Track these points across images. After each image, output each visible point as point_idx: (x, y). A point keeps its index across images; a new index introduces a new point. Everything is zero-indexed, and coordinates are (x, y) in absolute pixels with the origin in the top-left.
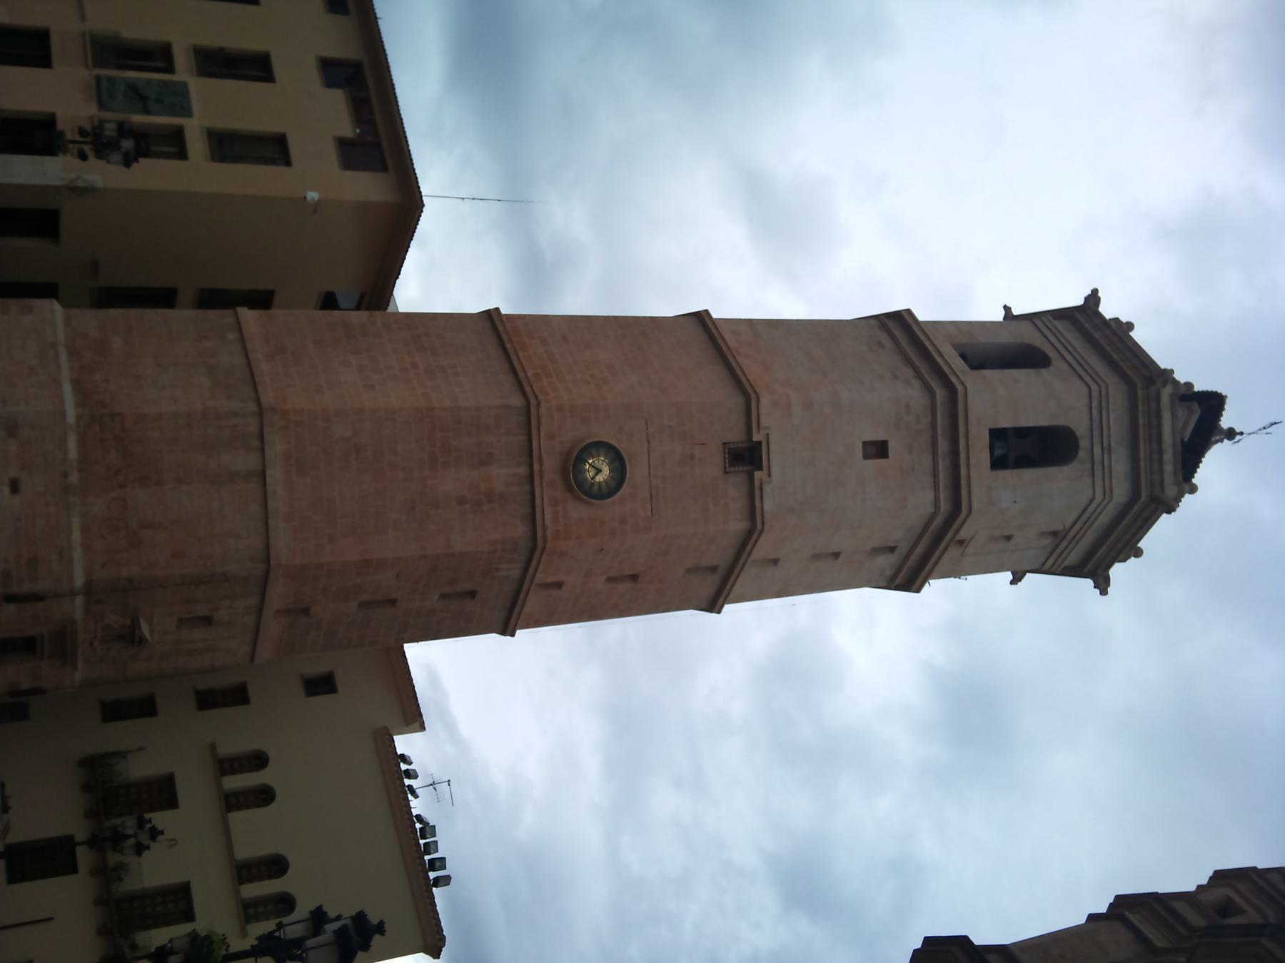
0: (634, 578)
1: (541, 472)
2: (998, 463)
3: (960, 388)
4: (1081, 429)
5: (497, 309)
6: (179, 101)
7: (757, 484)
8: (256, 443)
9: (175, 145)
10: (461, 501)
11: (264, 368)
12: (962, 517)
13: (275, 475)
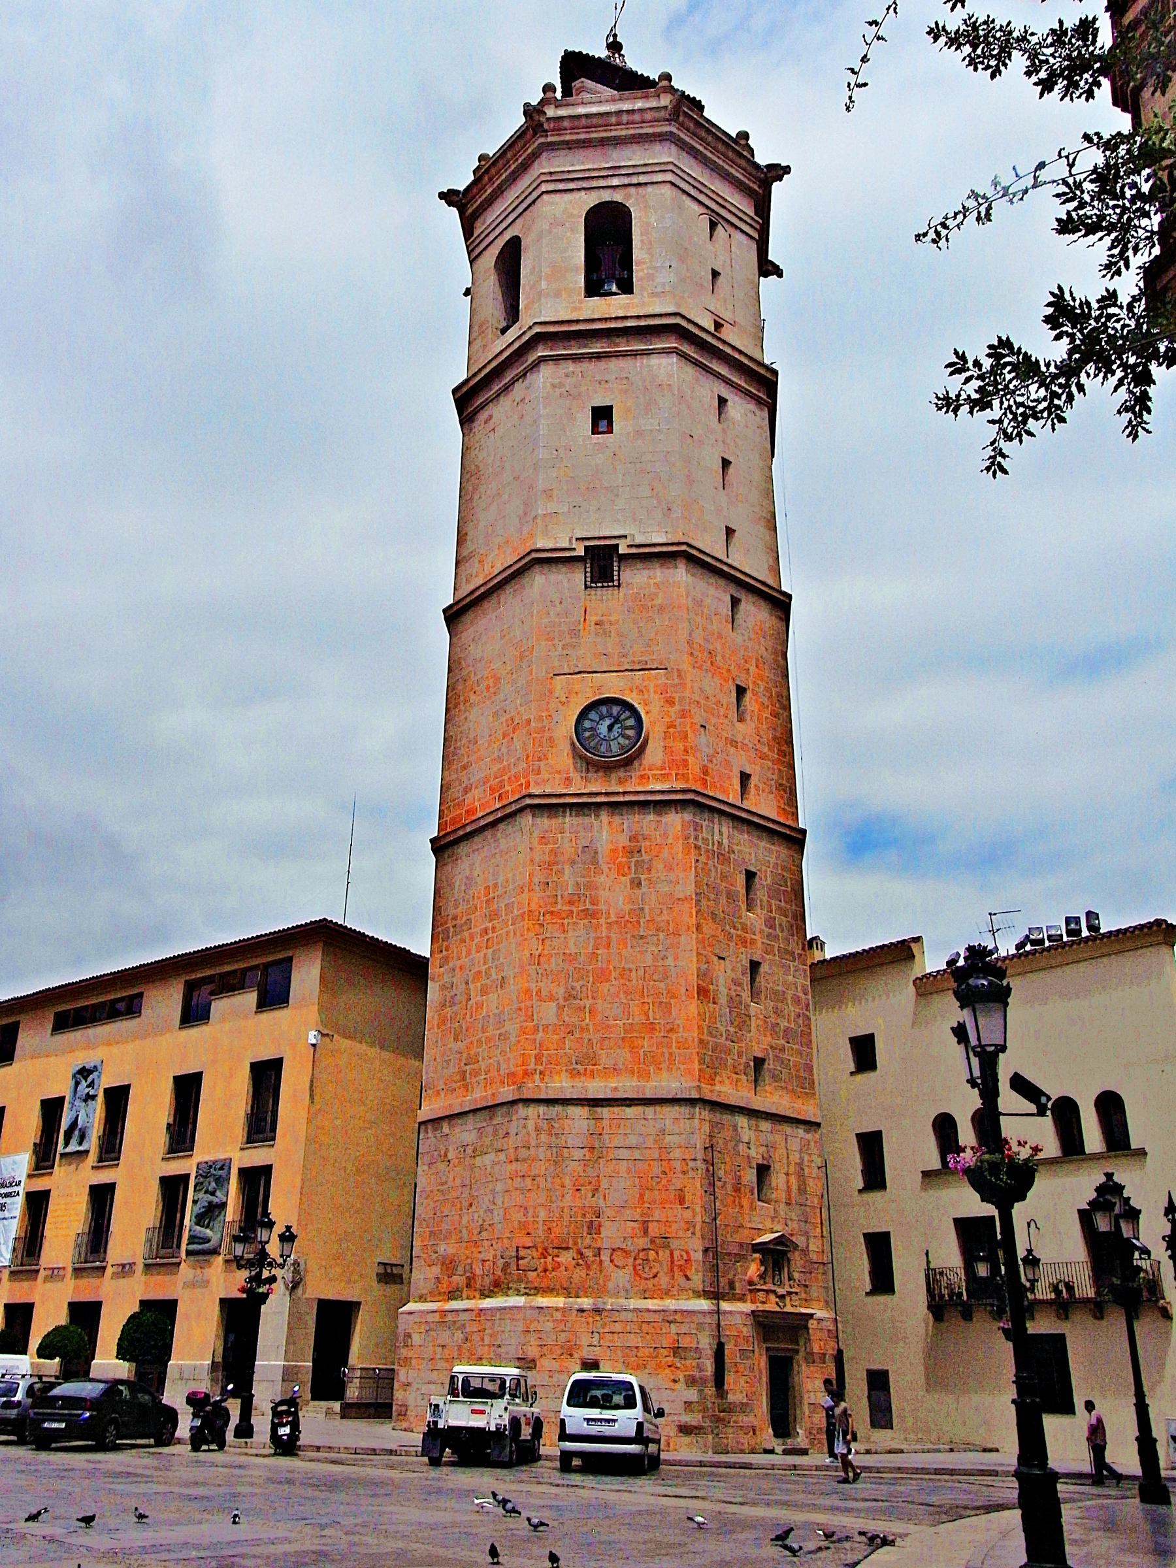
0: (741, 691)
1: (607, 794)
2: (627, 287)
3: (537, 329)
4: (592, 200)
5: (432, 841)
6: (214, 1173)
7: (634, 551)
9: (256, 1181)
11: (478, 1096)
12: (684, 323)
13: (596, 1088)
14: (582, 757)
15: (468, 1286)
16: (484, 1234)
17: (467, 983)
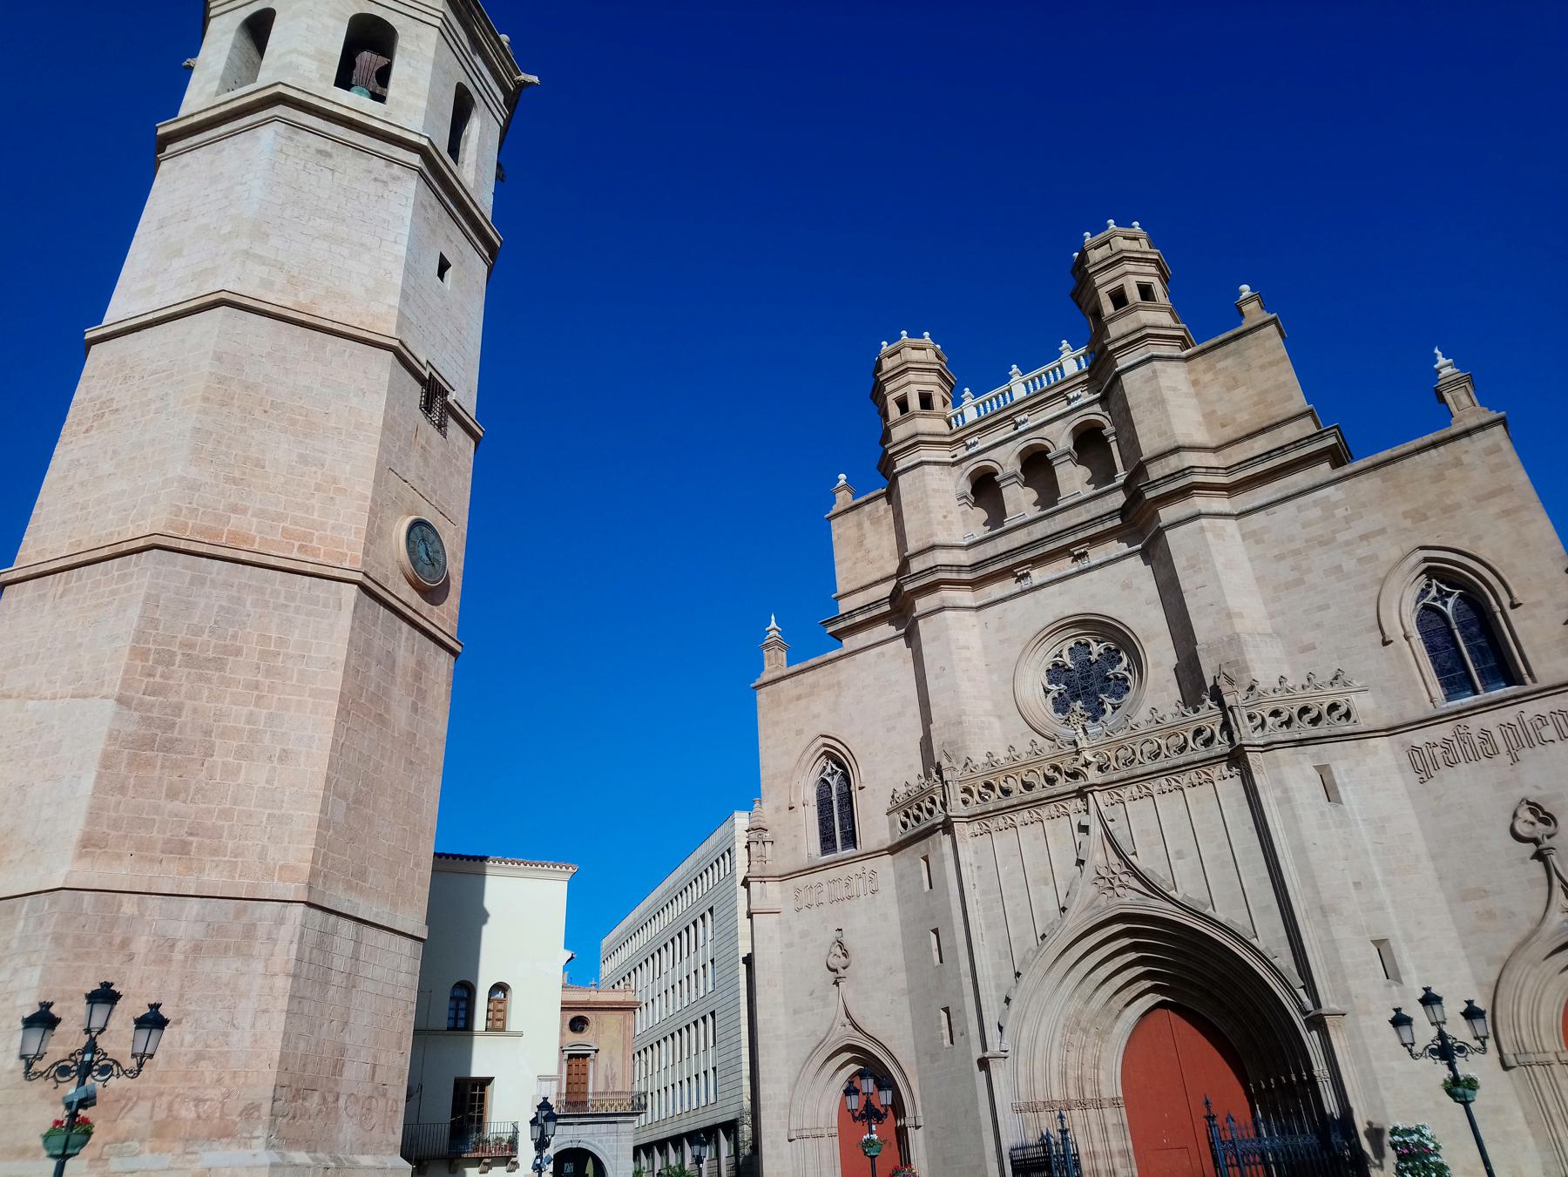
10: (415, 709)
11: (214, 879)
16: (203, 1063)
17: (208, 733)
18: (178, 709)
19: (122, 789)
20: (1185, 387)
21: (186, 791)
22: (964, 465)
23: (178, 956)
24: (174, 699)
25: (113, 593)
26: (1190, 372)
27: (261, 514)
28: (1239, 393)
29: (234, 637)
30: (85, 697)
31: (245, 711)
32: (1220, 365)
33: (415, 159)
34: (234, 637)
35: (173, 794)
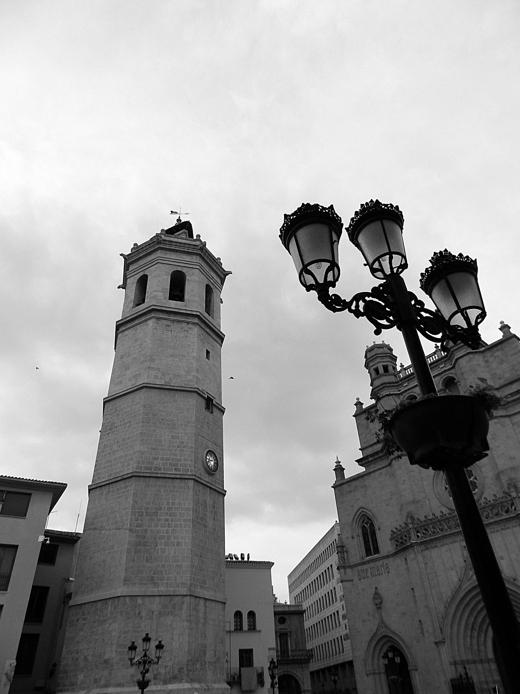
8: (198, 599)
11: (162, 589)
14: (204, 467)
15: (155, 678)
17: (155, 538)
18: (146, 531)
19: (134, 561)
20: (483, 363)
21: (151, 559)
22: (404, 394)
23: (155, 617)
24: (145, 528)
25: (123, 492)
26: (484, 357)
27: (162, 459)
28: (504, 366)
29: (159, 504)
30: (119, 529)
31: (165, 529)
32: (496, 354)
33: (196, 320)
34: (159, 504)
35: (148, 561)
